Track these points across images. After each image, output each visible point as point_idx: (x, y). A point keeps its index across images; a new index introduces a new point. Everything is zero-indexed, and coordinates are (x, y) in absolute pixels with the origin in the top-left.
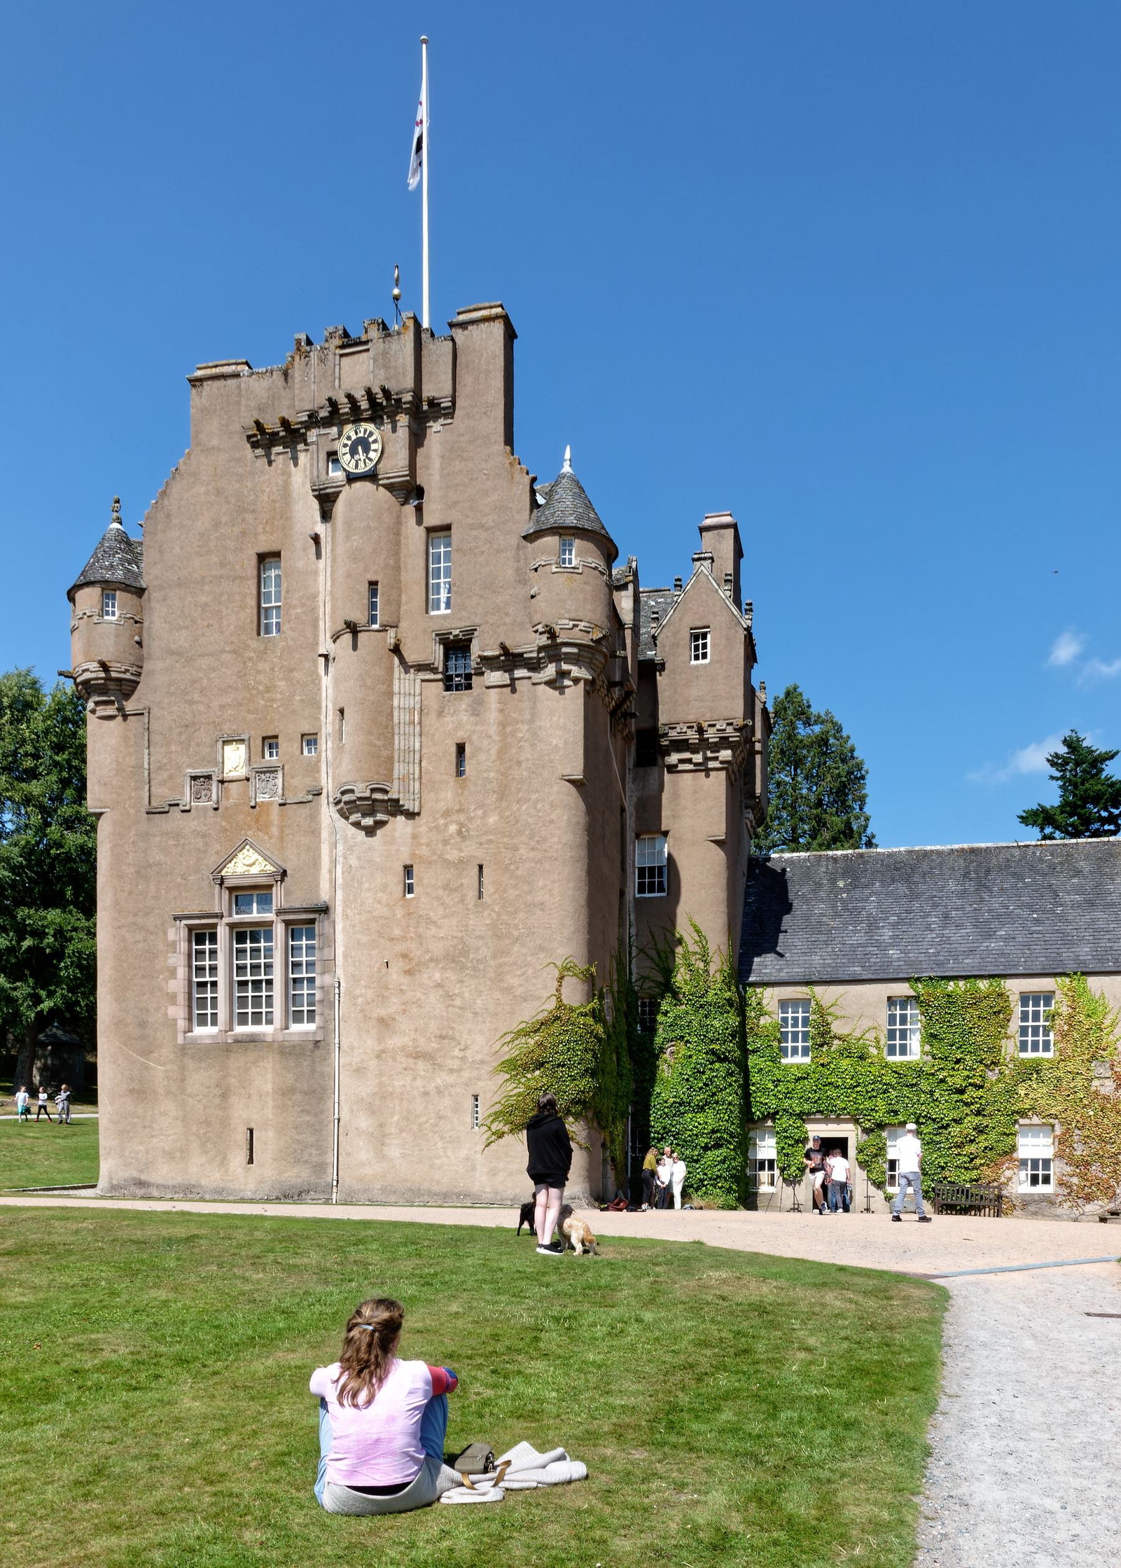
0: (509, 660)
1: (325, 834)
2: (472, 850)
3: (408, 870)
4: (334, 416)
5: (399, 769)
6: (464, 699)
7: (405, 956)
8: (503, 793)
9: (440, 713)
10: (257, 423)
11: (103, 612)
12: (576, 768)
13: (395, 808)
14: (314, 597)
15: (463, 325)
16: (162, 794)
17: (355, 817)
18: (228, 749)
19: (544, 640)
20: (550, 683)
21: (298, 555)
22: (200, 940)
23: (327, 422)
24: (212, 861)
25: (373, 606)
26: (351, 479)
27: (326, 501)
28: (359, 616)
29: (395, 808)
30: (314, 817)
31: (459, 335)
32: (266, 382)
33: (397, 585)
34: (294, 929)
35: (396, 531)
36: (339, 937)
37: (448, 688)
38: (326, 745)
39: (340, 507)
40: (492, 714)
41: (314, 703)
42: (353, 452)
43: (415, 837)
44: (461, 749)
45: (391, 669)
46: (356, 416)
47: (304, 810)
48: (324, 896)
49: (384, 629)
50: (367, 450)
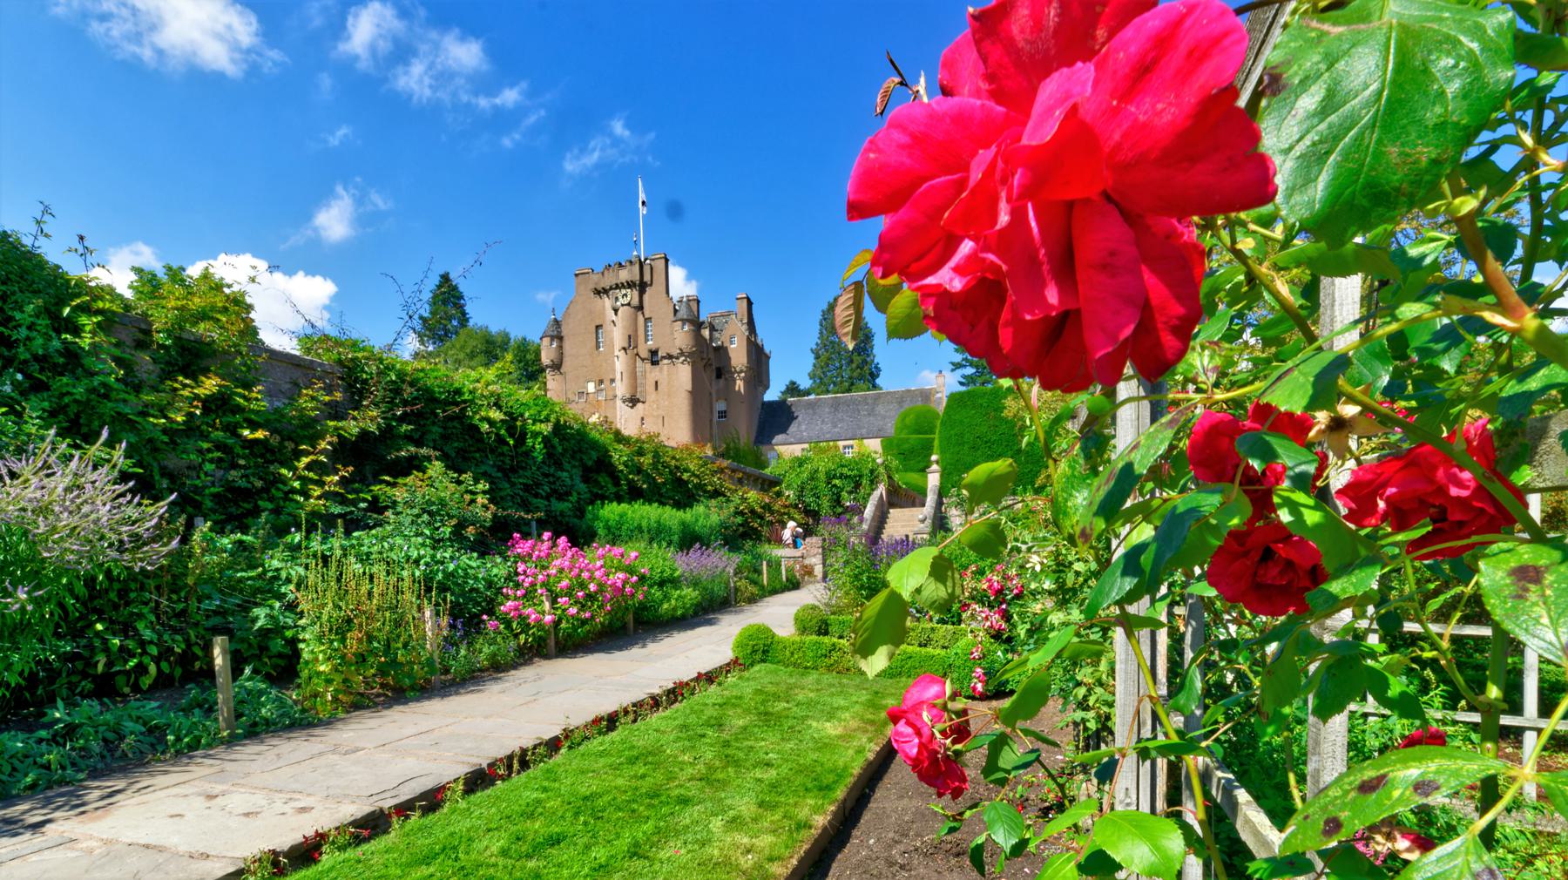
0: (670, 357)
2: (661, 412)
4: (617, 287)
6: (657, 368)
8: (669, 396)
12: (689, 387)
21: (608, 326)
27: (616, 311)
28: (626, 345)
29: (638, 401)
33: (636, 336)
35: (636, 320)
38: (618, 383)
40: (665, 372)
41: (614, 370)
46: (623, 286)
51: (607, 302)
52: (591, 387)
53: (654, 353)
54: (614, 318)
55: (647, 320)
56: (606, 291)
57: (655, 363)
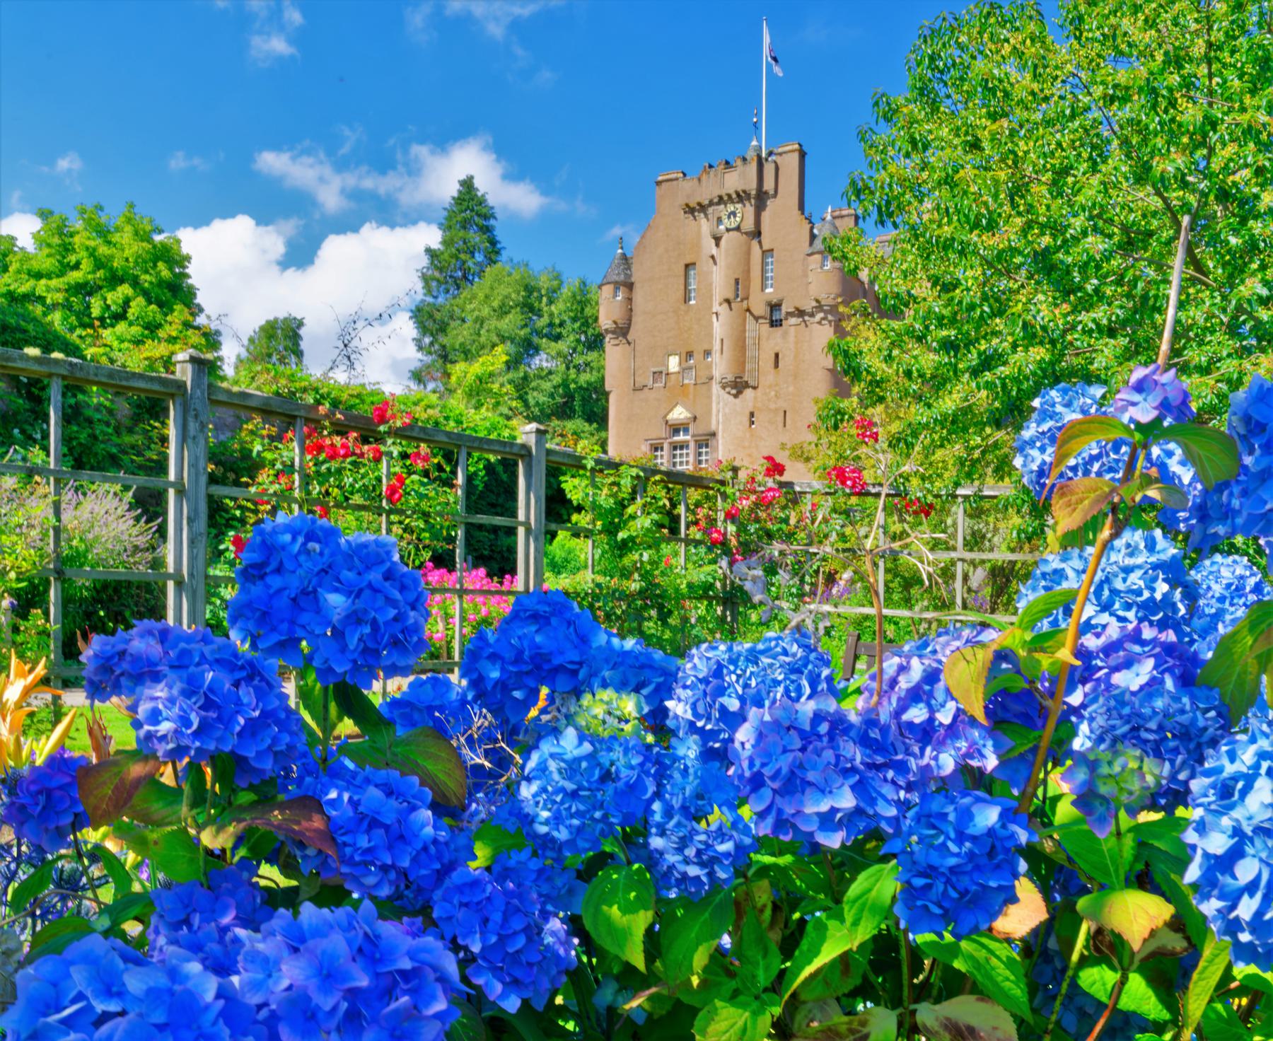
0: (800, 313)
1: (714, 398)
2: (782, 404)
3: (752, 415)
5: (748, 367)
6: (778, 331)
7: (750, 455)
9: (768, 338)
10: (687, 205)
11: (615, 296)
13: (747, 385)
14: (711, 284)
15: (780, 154)
16: (640, 381)
17: (728, 389)
18: (671, 358)
19: (814, 304)
20: (819, 323)
21: (704, 265)
22: (656, 450)
23: (719, 203)
24: (663, 412)
25: (737, 289)
26: (728, 230)
27: (717, 240)
28: (731, 296)
30: (710, 390)
31: (778, 159)
32: (690, 184)
34: (700, 445)
35: (748, 253)
36: (720, 447)
37: (772, 326)
39: (723, 242)
40: (791, 338)
42: (729, 217)
43: (755, 398)
44: (777, 355)
45: (745, 320)
47: (705, 387)
48: (713, 427)
49: (742, 301)
50: (735, 216)
51: (705, 226)
52: (674, 364)
53: (774, 307)
54: (714, 251)
55: (767, 253)
56: (703, 208)
57: (775, 324)
